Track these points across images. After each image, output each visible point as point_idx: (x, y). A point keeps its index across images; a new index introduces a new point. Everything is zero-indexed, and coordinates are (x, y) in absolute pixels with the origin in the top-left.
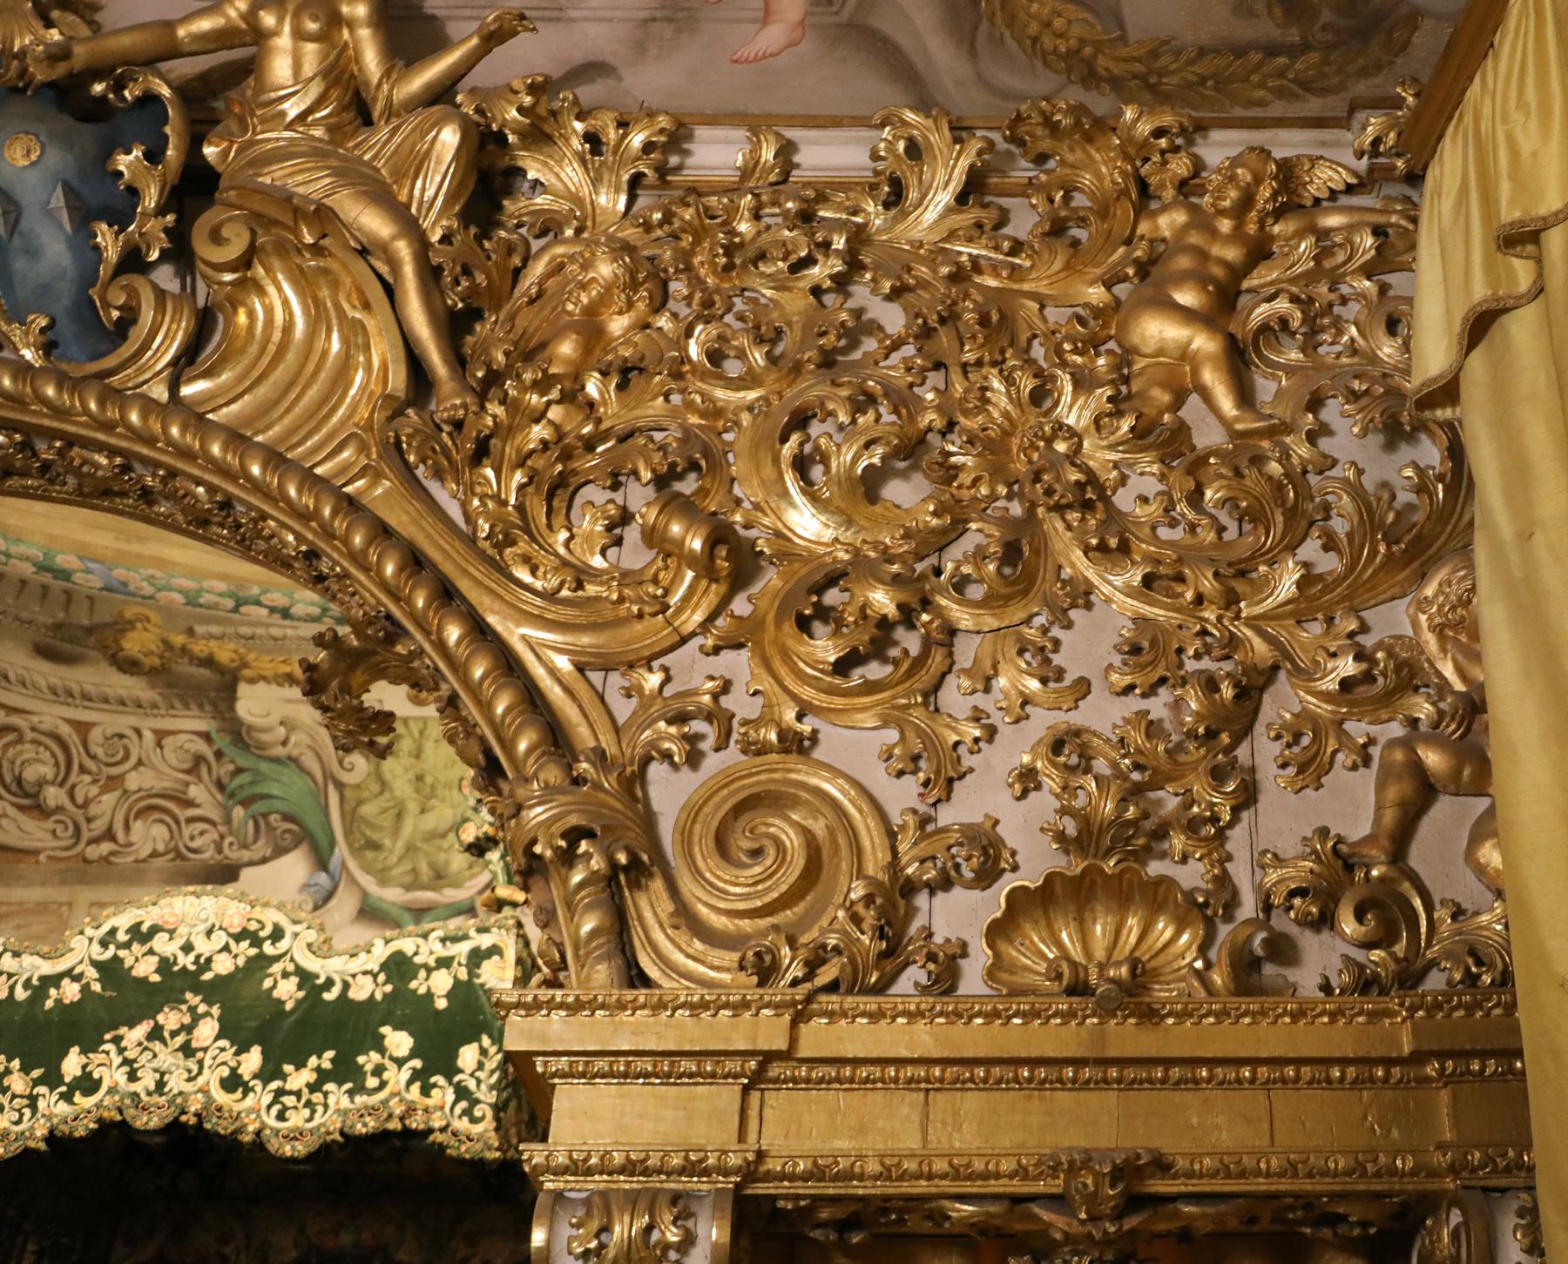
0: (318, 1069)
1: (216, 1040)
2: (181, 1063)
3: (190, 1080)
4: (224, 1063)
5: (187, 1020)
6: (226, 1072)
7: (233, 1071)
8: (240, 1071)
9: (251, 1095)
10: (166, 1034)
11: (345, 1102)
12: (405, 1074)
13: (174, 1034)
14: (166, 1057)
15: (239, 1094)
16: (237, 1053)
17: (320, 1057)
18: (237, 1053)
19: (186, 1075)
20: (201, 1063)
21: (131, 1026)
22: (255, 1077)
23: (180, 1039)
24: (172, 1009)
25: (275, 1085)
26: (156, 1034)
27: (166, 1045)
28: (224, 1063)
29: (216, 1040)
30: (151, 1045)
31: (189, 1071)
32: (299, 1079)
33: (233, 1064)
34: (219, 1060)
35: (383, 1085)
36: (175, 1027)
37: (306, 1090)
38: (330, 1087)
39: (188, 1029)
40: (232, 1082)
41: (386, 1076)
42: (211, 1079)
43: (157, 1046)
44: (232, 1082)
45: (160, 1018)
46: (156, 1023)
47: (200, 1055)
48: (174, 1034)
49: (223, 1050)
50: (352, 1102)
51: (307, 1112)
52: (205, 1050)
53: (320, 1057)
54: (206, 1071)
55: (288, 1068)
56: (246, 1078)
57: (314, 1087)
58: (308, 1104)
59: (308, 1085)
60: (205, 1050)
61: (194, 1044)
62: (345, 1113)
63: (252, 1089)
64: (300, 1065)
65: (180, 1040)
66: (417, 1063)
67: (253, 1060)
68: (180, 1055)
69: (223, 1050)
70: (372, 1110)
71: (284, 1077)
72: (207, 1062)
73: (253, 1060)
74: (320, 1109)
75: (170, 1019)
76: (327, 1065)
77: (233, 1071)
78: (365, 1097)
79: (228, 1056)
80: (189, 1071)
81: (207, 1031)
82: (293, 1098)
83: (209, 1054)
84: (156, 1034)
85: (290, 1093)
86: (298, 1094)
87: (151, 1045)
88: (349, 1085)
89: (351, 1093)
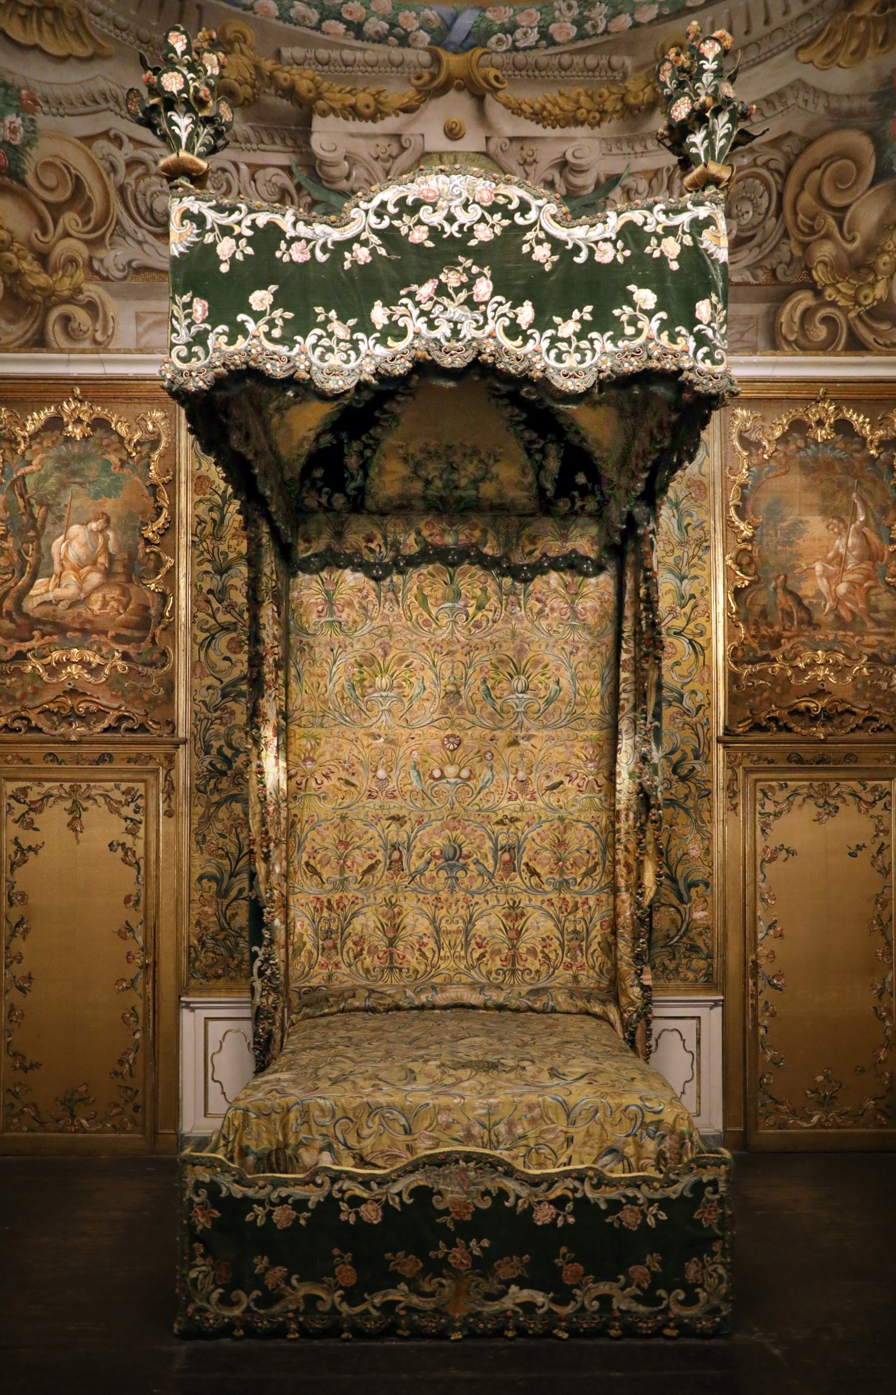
0: (581, 321)
1: (492, 296)
2: (469, 314)
3: (478, 328)
4: (504, 315)
5: (465, 279)
6: (507, 323)
7: (513, 321)
8: (518, 321)
9: (531, 341)
10: (451, 291)
11: (609, 347)
12: (655, 325)
13: (458, 290)
14: (456, 311)
15: (519, 342)
16: (513, 307)
17: (581, 311)
18: (513, 307)
19: (475, 325)
20: (484, 314)
21: (421, 284)
22: (531, 326)
23: (463, 295)
24: (450, 270)
25: (549, 333)
26: (441, 290)
27: (452, 300)
28: (504, 315)
29: (492, 296)
30: (440, 300)
31: (477, 321)
32: (568, 328)
33: (511, 315)
34: (498, 313)
35: (639, 332)
36: (457, 285)
37: (574, 338)
38: (594, 335)
39: (469, 286)
40: (513, 331)
41: (640, 325)
42: (496, 327)
43: (446, 301)
44: (513, 331)
45: (442, 277)
46: (440, 281)
47: (482, 307)
48: (458, 290)
49: (500, 304)
50: (616, 346)
51: (578, 356)
52: (486, 303)
53: (581, 311)
54: (490, 321)
55: (557, 320)
56: (524, 327)
57: (580, 336)
58: (578, 349)
59: (575, 333)
60: (486, 303)
61: (475, 299)
62: (612, 355)
63: (531, 336)
64: (567, 317)
65: (463, 295)
66: (663, 315)
67: (526, 313)
68: (466, 308)
69: (500, 304)
70: (635, 353)
71: (556, 327)
72: (490, 314)
73: (526, 313)
74: (589, 353)
75: (452, 279)
76: (588, 317)
77: (513, 321)
78: (626, 342)
79: (505, 309)
80: (477, 321)
81: (483, 288)
82: (565, 344)
83: (490, 308)
84: (441, 290)
85: (563, 340)
86: (568, 340)
87: (440, 300)
88: (609, 333)
89: (614, 340)
